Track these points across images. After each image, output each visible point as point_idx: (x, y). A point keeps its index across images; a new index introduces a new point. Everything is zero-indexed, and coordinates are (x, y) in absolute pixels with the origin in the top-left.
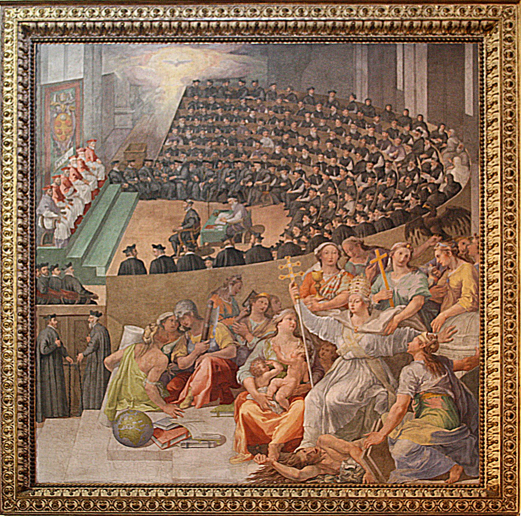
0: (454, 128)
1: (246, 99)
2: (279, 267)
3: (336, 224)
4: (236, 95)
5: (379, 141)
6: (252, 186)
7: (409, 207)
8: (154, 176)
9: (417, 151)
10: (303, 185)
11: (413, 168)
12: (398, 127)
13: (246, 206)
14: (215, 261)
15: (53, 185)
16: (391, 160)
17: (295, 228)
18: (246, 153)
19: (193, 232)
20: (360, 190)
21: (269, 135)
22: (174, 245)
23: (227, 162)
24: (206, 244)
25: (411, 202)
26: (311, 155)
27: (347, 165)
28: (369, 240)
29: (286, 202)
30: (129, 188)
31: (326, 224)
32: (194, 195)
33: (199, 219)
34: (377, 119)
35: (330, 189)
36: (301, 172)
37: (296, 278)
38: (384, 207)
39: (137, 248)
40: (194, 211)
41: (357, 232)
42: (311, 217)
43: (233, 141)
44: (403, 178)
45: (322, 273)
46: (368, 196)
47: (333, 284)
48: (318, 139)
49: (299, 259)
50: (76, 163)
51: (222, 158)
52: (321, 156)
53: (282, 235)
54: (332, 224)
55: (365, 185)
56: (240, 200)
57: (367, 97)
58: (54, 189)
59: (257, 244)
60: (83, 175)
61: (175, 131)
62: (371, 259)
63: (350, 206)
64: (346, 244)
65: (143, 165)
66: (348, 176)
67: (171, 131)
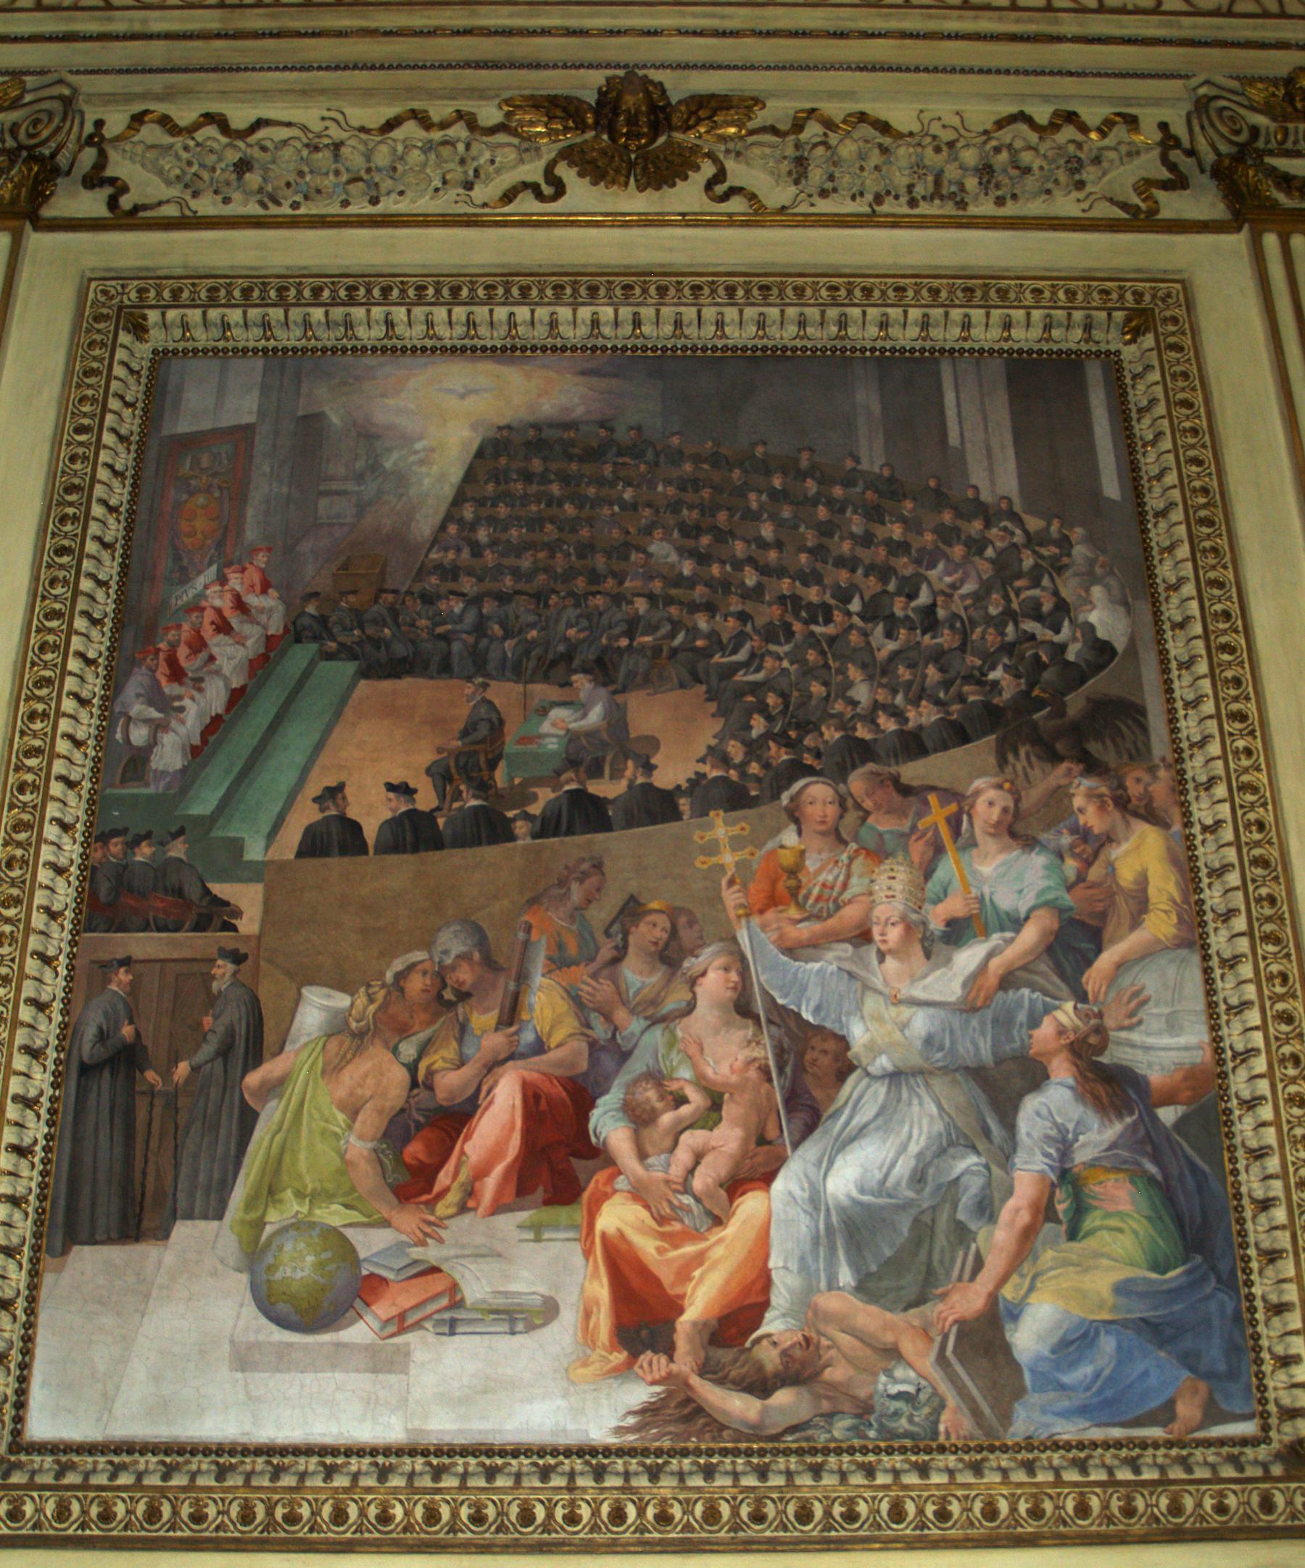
0: (1082, 525)
2: (696, 838)
3: (831, 734)
4: (593, 454)
5: (919, 550)
6: (630, 645)
7: (1000, 694)
8: (398, 626)
10: (748, 646)
12: (959, 523)
13: (615, 692)
14: (538, 824)
15: (163, 645)
16: (948, 591)
17: (732, 742)
18: (614, 574)
19: (487, 753)
20: (883, 655)
21: (667, 537)
23: (571, 594)
24: (517, 781)
25: (1004, 683)
27: (848, 600)
28: (912, 772)
29: (708, 684)
30: (339, 651)
31: (808, 733)
32: (492, 666)
33: (501, 722)
34: (909, 504)
35: (812, 656)
36: (743, 617)
37: (737, 863)
38: (942, 695)
39: (348, 791)
40: (490, 703)
41: (882, 754)
42: (769, 718)
43: (586, 549)
44: (979, 630)
45: (802, 853)
46: (901, 670)
47: (830, 878)
48: (779, 545)
49: (745, 818)
50: (221, 597)
51: (559, 587)
52: (787, 581)
53: (702, 760)
54: (821, 734)
55: (892, 646)
59: (640, 780)
60: (234, 623)
61: (452, 529)
62: (920, 815)
63: (862, 693)
64: (857, 782)
65: (376, 602)
66: (851, 627)
67: (443, 527)
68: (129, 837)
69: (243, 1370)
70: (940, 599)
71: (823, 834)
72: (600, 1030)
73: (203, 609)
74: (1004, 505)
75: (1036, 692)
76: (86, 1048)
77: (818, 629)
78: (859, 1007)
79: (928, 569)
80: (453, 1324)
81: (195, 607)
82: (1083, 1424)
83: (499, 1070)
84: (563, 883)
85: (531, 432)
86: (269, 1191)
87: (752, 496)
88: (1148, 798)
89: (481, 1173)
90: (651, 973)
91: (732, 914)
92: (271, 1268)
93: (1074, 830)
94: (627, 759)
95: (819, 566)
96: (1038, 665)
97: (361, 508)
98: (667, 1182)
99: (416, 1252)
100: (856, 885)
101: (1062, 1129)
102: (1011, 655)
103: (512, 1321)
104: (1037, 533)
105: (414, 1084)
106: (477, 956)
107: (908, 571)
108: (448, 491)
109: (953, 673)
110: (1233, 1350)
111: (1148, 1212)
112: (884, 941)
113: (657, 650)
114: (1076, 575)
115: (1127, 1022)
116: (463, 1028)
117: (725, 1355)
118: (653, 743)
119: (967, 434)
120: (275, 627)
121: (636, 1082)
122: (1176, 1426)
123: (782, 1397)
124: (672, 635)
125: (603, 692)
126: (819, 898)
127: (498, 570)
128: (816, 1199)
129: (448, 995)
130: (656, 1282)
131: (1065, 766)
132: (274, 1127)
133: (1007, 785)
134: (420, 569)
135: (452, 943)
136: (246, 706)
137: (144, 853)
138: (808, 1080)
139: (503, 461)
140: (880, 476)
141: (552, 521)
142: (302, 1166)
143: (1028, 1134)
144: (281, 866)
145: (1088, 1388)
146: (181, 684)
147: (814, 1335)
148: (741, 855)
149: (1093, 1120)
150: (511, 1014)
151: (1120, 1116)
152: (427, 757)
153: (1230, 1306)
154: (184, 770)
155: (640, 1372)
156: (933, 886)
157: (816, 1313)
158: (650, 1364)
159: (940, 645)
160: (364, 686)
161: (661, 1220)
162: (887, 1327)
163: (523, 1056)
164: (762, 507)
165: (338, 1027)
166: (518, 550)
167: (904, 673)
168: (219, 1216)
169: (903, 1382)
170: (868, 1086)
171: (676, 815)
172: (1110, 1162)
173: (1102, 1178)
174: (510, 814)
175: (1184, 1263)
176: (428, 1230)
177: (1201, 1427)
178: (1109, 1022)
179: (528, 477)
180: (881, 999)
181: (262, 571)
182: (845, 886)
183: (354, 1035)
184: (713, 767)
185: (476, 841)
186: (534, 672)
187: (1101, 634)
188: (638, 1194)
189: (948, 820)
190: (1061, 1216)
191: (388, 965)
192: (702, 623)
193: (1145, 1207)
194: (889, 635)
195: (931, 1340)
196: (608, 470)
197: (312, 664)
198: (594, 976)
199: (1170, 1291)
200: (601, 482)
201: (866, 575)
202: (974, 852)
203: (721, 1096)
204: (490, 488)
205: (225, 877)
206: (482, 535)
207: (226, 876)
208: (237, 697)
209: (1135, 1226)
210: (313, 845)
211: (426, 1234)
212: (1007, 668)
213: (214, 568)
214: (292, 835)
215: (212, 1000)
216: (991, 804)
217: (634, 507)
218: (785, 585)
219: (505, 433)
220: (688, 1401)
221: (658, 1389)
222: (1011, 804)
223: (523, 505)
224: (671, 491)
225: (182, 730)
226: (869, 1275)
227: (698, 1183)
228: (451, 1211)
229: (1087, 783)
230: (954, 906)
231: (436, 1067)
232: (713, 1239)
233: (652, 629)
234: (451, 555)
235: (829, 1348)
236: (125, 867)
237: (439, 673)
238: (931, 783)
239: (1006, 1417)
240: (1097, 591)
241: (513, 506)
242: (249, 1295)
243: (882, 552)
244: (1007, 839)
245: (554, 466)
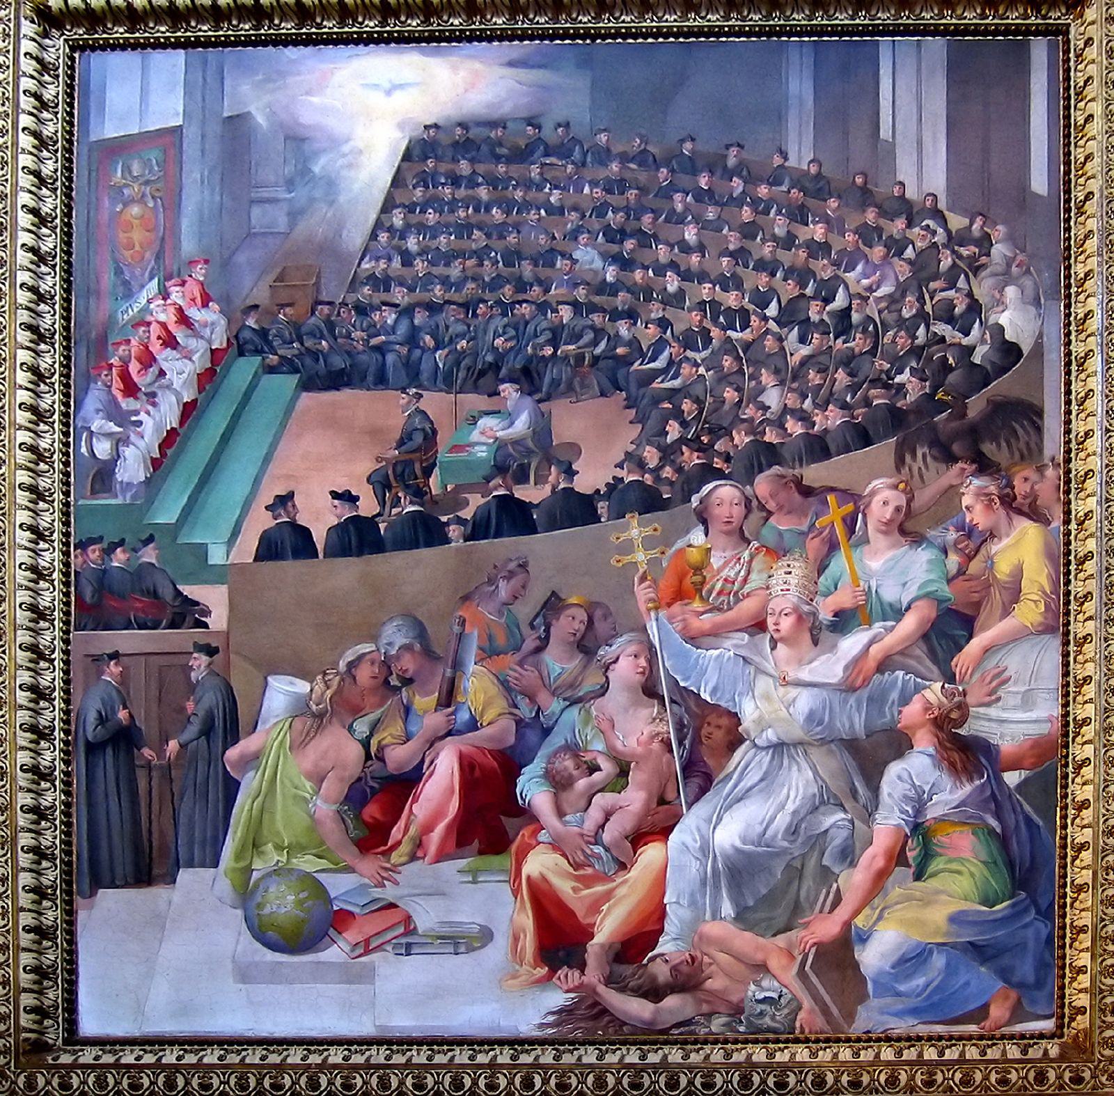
1: (543, 165)
3: (741, 438)
9: (924, 274)
10: (666, 354)
12: (882, 222)
13: (539, 401)
15: (114, 361)
17: (648, 448)
18: (540, 282)
20: (794, 361)
23: (499, 303)
25: (909, 386)
28: (814, 474)
32: (425, 376)
33: (435, 432)
35: (727, 362)
36: (664, 324)
42: (684, 424)
43: (511, 257)
47: (732, 574)
48: (701, 248)
51: (487, 295)
53: (620, 466)
54: (732, 439)
55: (805, 351)
56: (526, 386)
61: (383, 237)
63: (772, 398)
64: (763, 484)
65: (313, 313)
66: (767, 331)
67: (374, 236)
68: (105, 545)
69: (245, 983)
71: (728, 533)
72: (526, 711)
73: (149, 324)
76: (90, 729)
78: (751, 689)
80: (409, 946)
82: (911, 1021)
83: (438, 745)
84: (491, 581)
86: (254, 844)
87: (678, 197)
88: (1033, 497)
89: (428, 829)
90: (571, 658)
91: (643, 608)
92: (260, 906)
93: (960, 528)
95: (740, 270)
96: (945, 368)
97: (294, 215)
98: (582, 835)
99: (377, 893)
100: (756, 580)
101: (920, 792)
103: (456, 944)
105: (368, 756)
106: (417, 647)
109: (861, 377)
110: (1043, 967)
111: (984, 856)
112: (778, 630)
113: (580, 358)
115: (988, 699)
116: (407, 710)
117: (627, 970)
118: (575, 449)
120: (219, 342)
121: (555, 754)
122: (987, 1024)
123: (671, 1001)
124: (595, 343)
125: (528, 401)
126: (720, 593)
127: (429, 279)
128: (706, 849)
129: (394, 681)
130: (572, 914)
131: (960, 465)
132: (253, 793)
135: (395, 636)
136: (198, 418)
137: (119, 558)
138: (704, 749)
139: (430, 163)
142: (279, 825)
143: (889, 795)
144: (241, 567)
145: (919, 995)
146: (136, 398)
147: (699, 955)
149: (947, 781)
150: (448, 698)
151: (971, 780)
152: (367, 466)
153: (1044, 932)
154: (148, 481)
155: (558, 983)
157: (700, 938)
158: (566, 976)
159: (852, 349)
160: (306, 399)
161: (577, 866)
162: (758, 948)
163: (459, 733)
165: (301, 708)
166: (449, 257)
167: (814, 377)
168: (216, 865)
169: (768, 990)
170: (755, 755)
172: (960, 818)
173: (950, 830)
174: (444, 519)
175: (1010, 898)
176: (385, 875)
177: (1009, 1023)
178: (970, 699)
180: (771, 681)
182: (745, 581)
183: (314, 715)
185: (415, 545)
186: (465, 380)
187: (1009, 336)
188: (556, 846)
189: (844, 520)
190: (911, 861)
191: (340, 656)
192: (623, 328)
193: (984, 856)
194: (803, 340)
195: (793, 957)
198: (521, 664)
199: (995, 921)
200: (528, 184)
201: (785, 279)
202: (866, 548)
203: (629, 764)
206: (412, 243)
208: (188, 410)
209: (973, 869)
210: (269, 549)
211: (383, 878)
215: (192, 688)
217: (561, 211)
218: (705, 291)
220: (596, 1004)
221: (572, 995)
223: (452, 211)
224: (598, 192)
225: (141, 444)
226: (747, 908)
227: (606, 837)
228: (404, 859)
230: (843, 598)
231: (384, 743)
232: (619, 880)
233: (575, 337)
234: (383, 264)
235: (711, 964)
236: (104, 571)
237: (376, 384)
239: (850, 1016)
240: (1011, 292)
242: (244, 925)
243: (802, 254)
245: (481, 168)
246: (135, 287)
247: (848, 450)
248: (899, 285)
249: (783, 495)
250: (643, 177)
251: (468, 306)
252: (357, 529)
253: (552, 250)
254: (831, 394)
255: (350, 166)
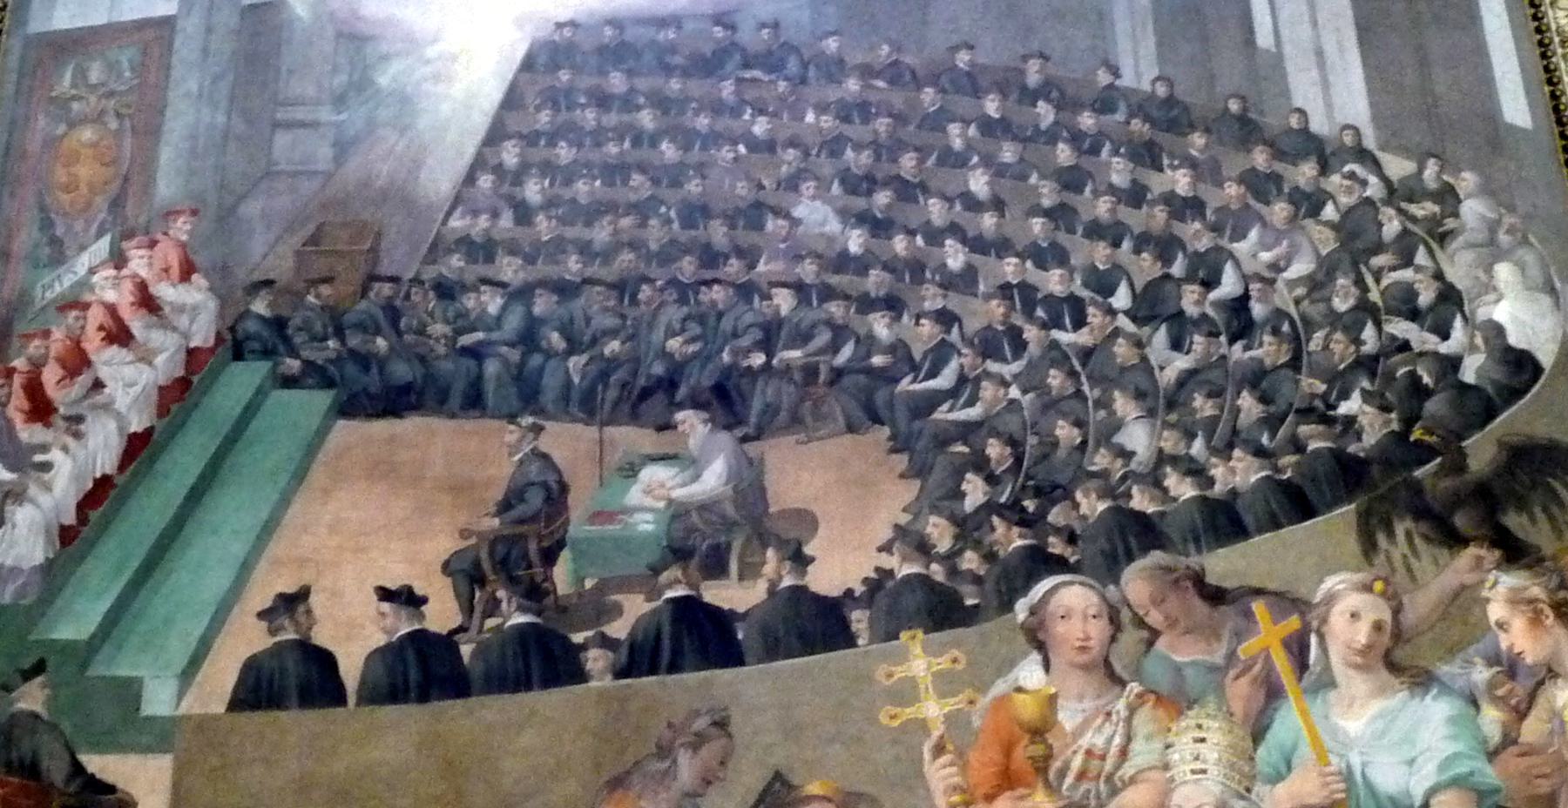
0: (1473, 168)
3: (1092, 505)
4: (708, 65)
5: (1218, 210)
6: (768, 364)
7: (1359, 439)
8: (399, 333)
11: (1351, 302)
12: (1279, 167)
13: (745, 439)
14: (624, 651)
16: (1267, 274)
17: (933, 519)
18: (740, 252)
19: (540, 538)
20: (1168, 376)
21: (822, 193)
22: (464, 588)
23: (673, 282)
24: (589, 584)
25: (1363, 420)
26: (977, 259)
27: (1110, 291)
29: (893, 425)
31: (1054, 503)
33: (564, 488)
34: (1198, 140)
35: (1055, 379)
36: (946, 318)
38: (1265, 440)
40: (545, 457)
41: (1175, 536)
42: (992, 479)
43: (696, 213)
44: (1319, 336)
45: (1052, 699)
46: (1198, 401)
48: (998, 205)
49: (958, 644)
50: (116, 286)
51: (654, 271)
52: (1014, 260)
53: (886, 548)
54: (1076, 506)
55: (1182, 363)
56: (722, 419)
57: (1155, 72)
58: (18, 380)
59: (787, 582)
61: (485, 181)
62: (1239, 636)
63: (1138, 437)
64: (1136, 582)
65: (364, 292)
66: (1116, 332)
67: (470, 179)
70: (1255, 287)
71: (1086, 668)
74: (1348, 139)
75: (1416, 434)
77: (1064, 337)
79: (1233, 239)
81: (74, 303)
84: (664, 751)
85: (608, 32)
87: (954, 129)
93: (1493, 659)
94: (765, 546)
95: (1062, 238)
96: (1418, 391)
97: (343, 148)
100: (1143, 753)
102: (1373, 375)
104: (1402, 180)
107: (1204, 243)
108: (480, 122)
113: (811, 372)
114: (1472, 246)
118: (807, 520)
119: (1285, 33)
120: (202, 334)
124: (834, 348)
125: (725, 439)
126: (1082, 775)
127: (558, 247)
131: (1472, 551)
133: (1379, 586)
134: (434, 246)
139: (564, 76)
140: (1152, 96)
141: (642, 168)
148: (952, 704)
152: (445, 544)
156: (1266, 754)
159: (1261, 361)
160: (346, 431)
164: (969, 146)
166: (592, 213)
167: (1203, 406)
171: (842, 637)
174: (578, 638)
179: (602, 101)
181: (183, 246)
182: (1124, 753)
184: (904, 559)
185: (521, 683)
187: (1515, 339)
189: (1286, 644)
192: (880, 326)
194: (1177, 345)
196: (727, 89)
197: (260, 393)
200: (717, 108)
201: (1137, 251)
202: (1332, 695)
204: (544, 117)
205: (100, 747)
206: (533, 191)
207: (108, 743)
212: (1367, 396)
213: (104, 243)
214: (222, 674)
216: (1354, 616)
218: (1010, 268)
219: (567, 32)
222: (1387, 616)
223: (598, 145)
224: (827, 121)
229: (1505, 583)
233: (802, 337)
234: (483, 222)
238: (1255, 583)
240: (1504, 272)
241: (580, 146)
243: (1160, 214)
244: (1385, 674)
246: (70, 247)
247: (1277, 526)
248: (1321, 261)
249: (1173, 603)
250: (898, 100)
251: (624, 288)
252: (419, 653)
253: (758, 206)
254: (1235, 432)
255: (437, 78)
